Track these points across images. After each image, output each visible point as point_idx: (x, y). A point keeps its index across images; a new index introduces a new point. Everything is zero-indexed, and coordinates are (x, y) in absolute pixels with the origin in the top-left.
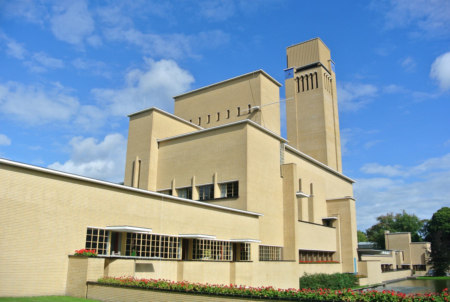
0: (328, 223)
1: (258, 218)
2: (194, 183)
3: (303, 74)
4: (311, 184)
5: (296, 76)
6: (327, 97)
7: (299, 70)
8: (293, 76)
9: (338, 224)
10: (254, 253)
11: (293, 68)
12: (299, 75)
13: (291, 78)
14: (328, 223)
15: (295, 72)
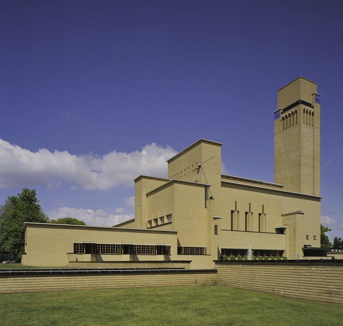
0: (281, 231)
1: (177, 234)
2: (165, 214)
3: (287, 113)
4: (263, 205)
5: (282, 116)
6: (305, 130)
7: (285, 110)
8: (279, 117)
9: (287, 231)
10: (174, 251)
11: (280, 110)
12: (284, 115)
13: (278, 118)
14: (281, 231)
15: (282, 113)
